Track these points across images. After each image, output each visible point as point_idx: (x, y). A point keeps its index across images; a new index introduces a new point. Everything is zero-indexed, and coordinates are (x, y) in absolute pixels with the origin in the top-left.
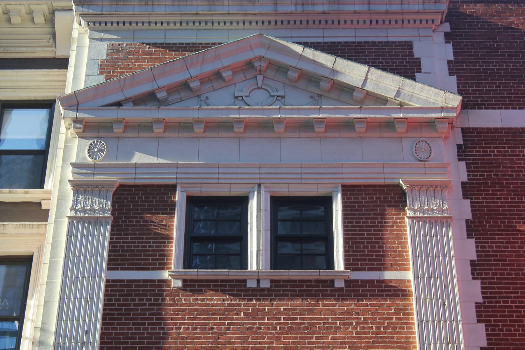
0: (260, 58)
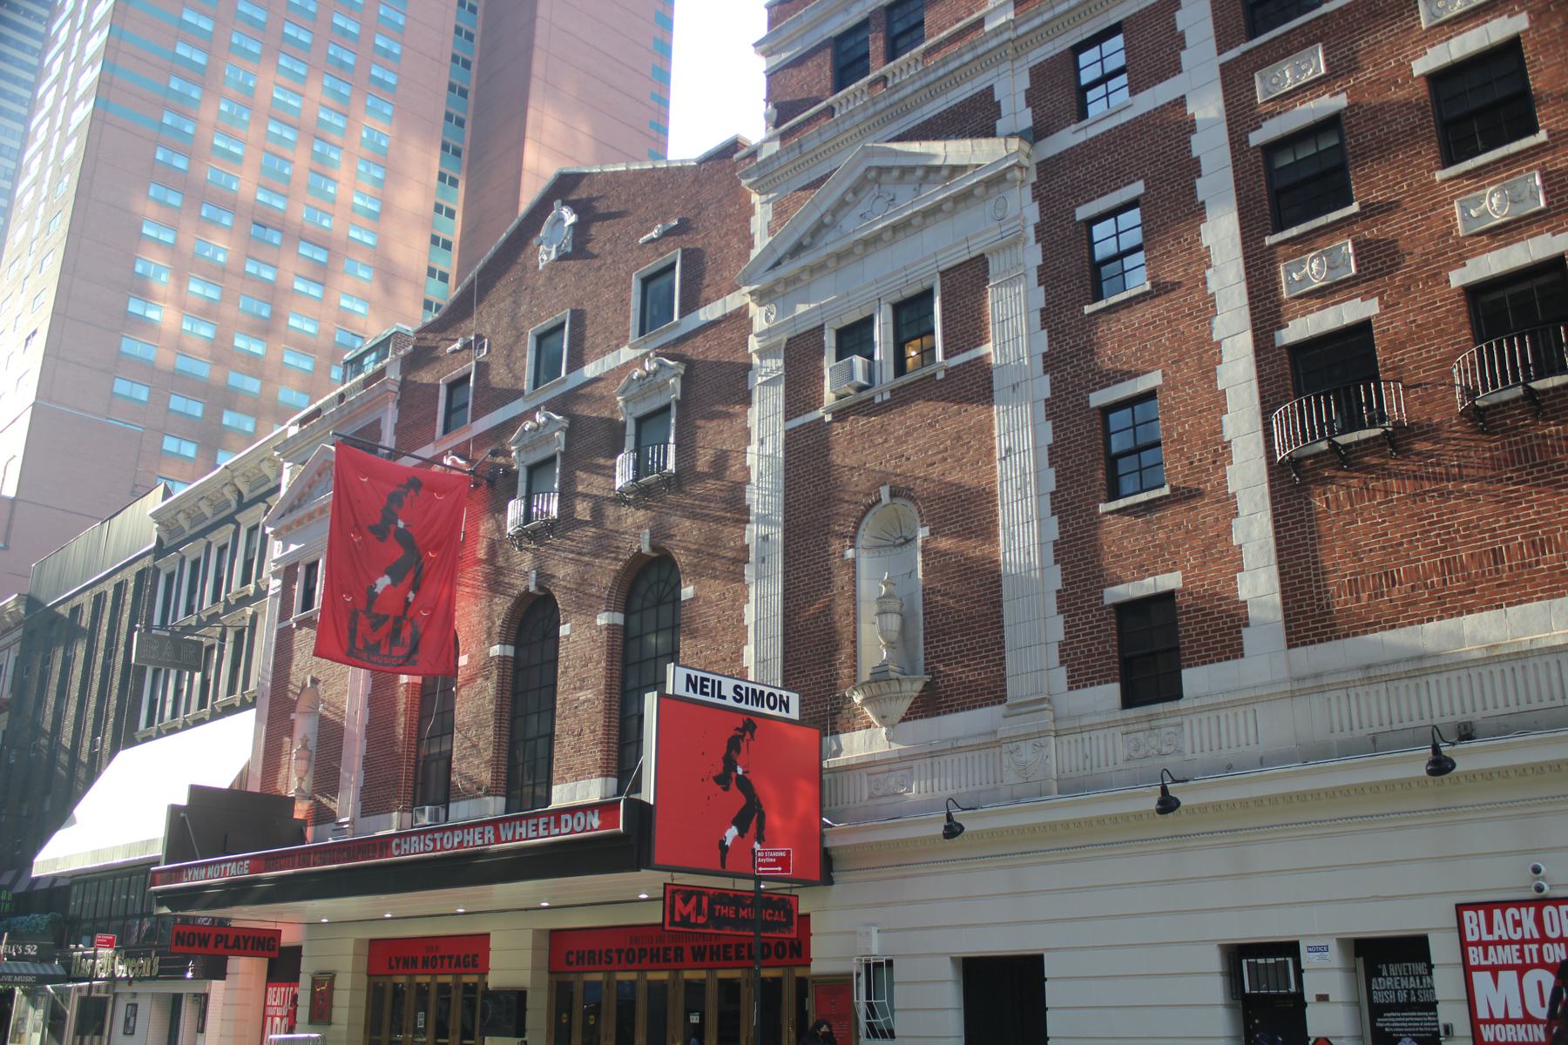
0: (869, 169)
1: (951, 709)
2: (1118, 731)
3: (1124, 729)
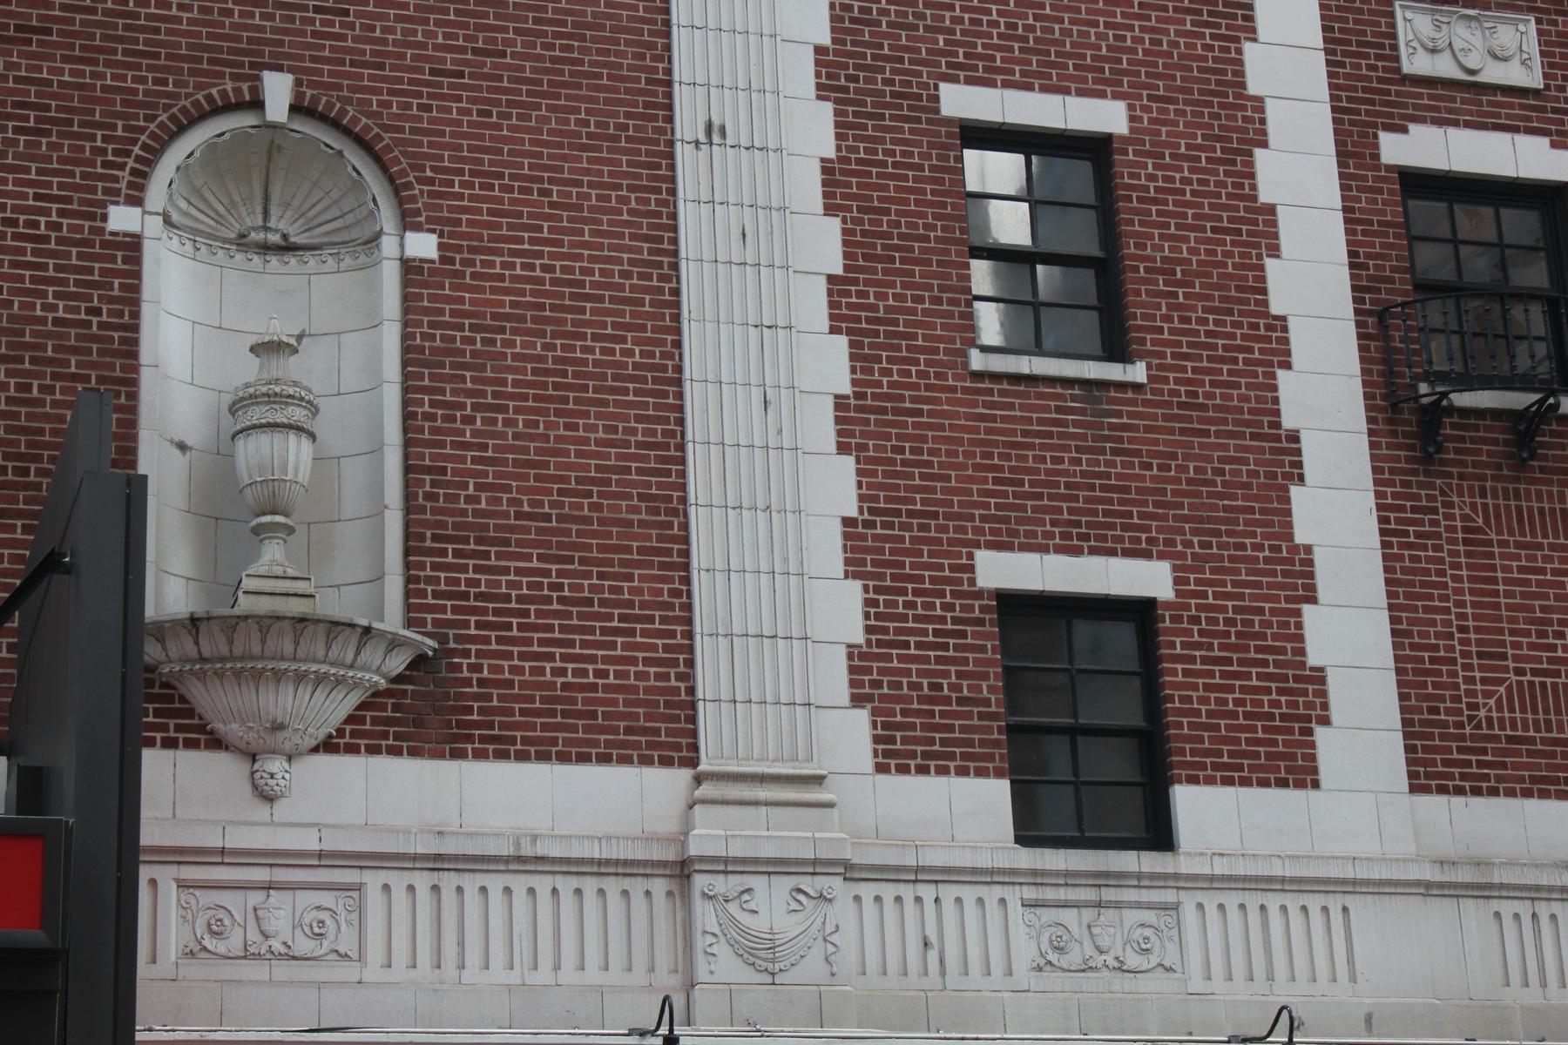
1: (501, 749)
2: (1013, 895)
3: (1030, 893)
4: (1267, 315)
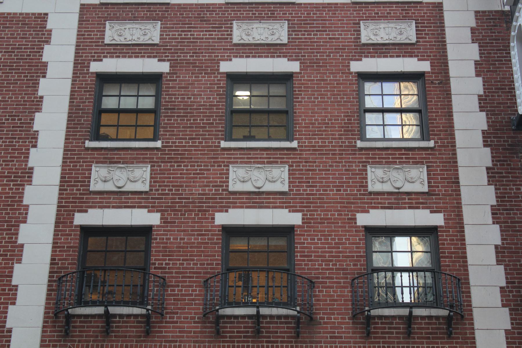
4: (10, 285)
